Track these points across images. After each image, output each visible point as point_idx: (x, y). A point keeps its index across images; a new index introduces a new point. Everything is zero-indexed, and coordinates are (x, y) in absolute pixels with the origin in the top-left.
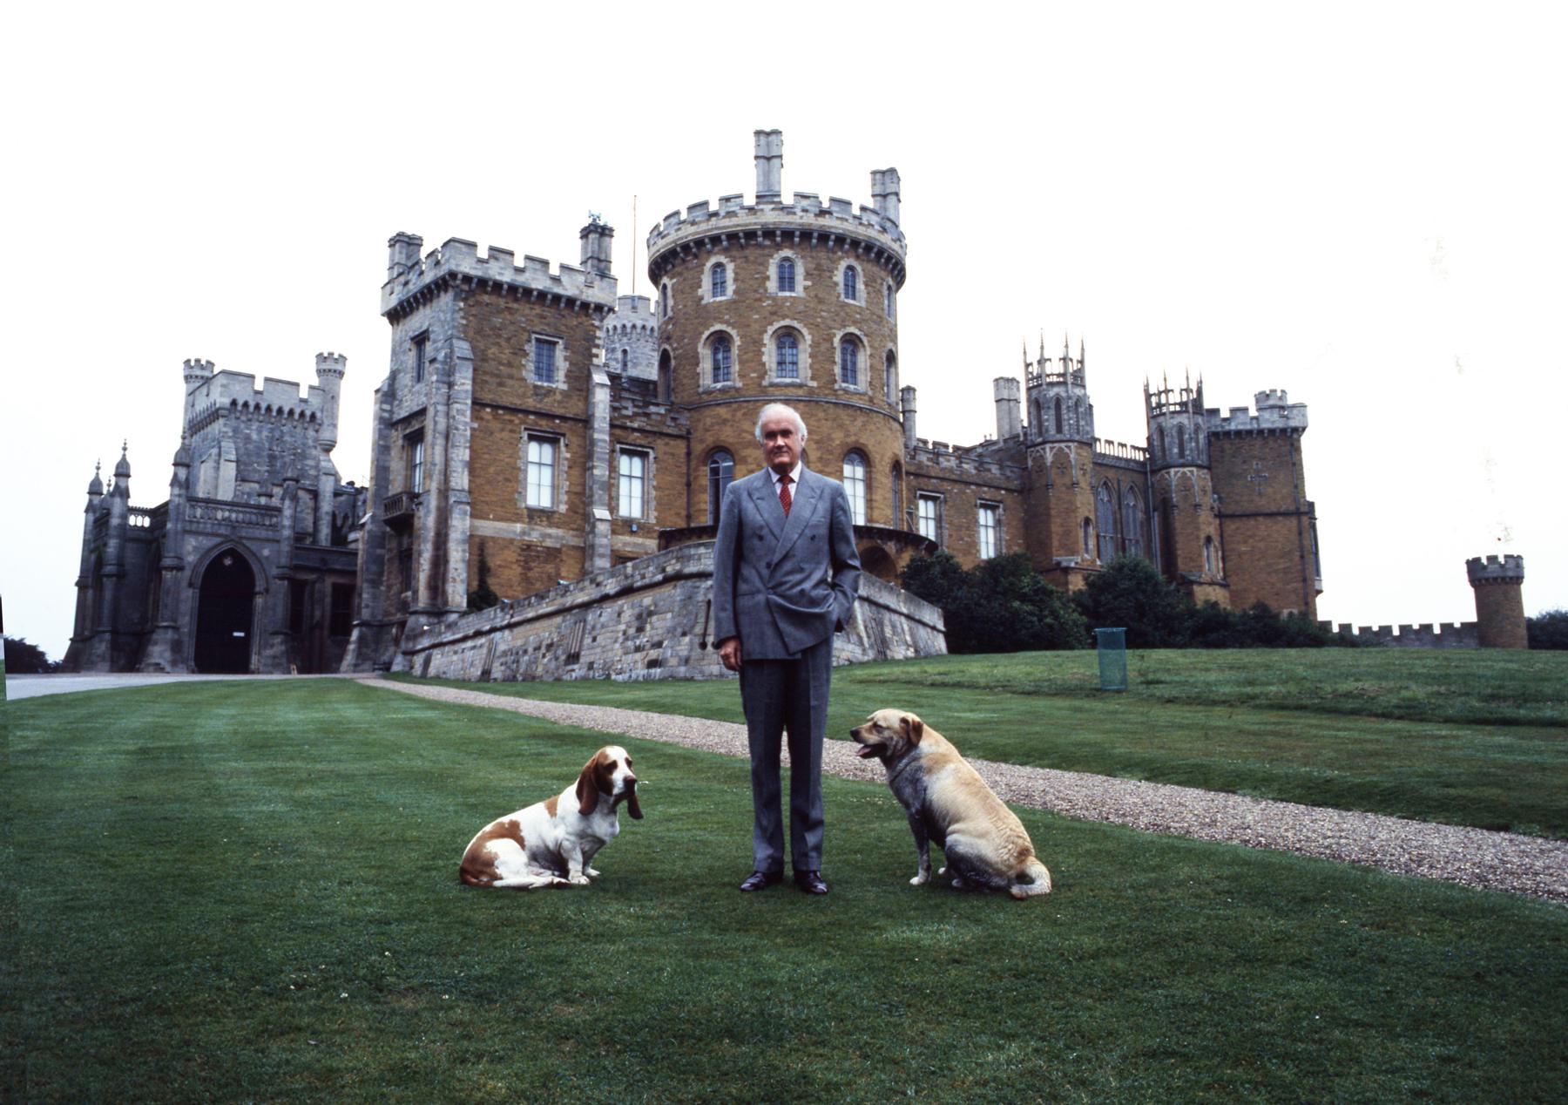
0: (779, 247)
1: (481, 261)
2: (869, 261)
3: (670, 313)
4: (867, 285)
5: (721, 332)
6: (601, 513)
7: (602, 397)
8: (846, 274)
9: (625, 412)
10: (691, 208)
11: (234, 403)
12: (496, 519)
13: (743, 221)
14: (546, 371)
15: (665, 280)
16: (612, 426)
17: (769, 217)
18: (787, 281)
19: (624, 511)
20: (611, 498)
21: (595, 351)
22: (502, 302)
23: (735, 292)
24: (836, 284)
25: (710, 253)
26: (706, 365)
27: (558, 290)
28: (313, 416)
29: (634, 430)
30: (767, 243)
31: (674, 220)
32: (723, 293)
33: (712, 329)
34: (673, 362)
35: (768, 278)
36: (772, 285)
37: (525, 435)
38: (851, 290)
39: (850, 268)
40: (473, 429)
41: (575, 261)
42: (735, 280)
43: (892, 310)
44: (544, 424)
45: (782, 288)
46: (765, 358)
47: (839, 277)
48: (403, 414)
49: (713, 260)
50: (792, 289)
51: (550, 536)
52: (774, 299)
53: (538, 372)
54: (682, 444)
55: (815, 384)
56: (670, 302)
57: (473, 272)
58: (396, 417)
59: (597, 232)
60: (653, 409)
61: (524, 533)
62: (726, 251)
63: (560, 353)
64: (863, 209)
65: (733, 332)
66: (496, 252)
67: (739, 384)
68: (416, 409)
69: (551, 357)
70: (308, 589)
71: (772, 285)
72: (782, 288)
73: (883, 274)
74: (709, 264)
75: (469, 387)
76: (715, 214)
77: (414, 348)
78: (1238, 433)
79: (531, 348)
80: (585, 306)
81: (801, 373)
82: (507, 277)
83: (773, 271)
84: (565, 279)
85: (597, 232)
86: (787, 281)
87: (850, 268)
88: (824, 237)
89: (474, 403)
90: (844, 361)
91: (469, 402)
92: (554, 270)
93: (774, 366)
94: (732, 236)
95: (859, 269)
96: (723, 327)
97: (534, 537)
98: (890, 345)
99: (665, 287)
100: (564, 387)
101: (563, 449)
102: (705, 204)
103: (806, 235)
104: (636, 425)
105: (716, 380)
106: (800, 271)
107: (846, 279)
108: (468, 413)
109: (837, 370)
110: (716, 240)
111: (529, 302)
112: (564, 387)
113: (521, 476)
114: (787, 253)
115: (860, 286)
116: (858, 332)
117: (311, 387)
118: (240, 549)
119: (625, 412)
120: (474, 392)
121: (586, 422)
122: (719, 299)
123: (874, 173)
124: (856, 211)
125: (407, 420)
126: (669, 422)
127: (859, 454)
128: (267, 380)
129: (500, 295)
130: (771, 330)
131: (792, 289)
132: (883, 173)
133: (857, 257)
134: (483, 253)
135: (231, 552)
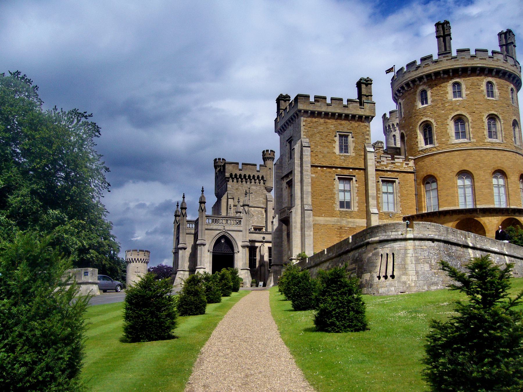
0: (452, 78)
1: (311, 103)
2: (500, 78)
3: (403, 116)
4: (499, 90)
5: (427, 121)
6: (373, 210)
7: (371, 159)
8: (487, 85)
9: (382, 163)
10: (408, 66)
11: (231, 175)
12: (325, 216)
13: (432, 68)
14: (344, 148)
15: (400, 101)
16: (376, 170)
17: (446, 65)
19: (385, 209)
20: (378, 203)
21: (366, 137)
22: (322, 121)
23: (432, 102)
24: (482, 91)
25: (419, 85)
27: (346, 112)
28: (263, 177)
29: (387, 171)
30: (446, 76)
31: (400, 72)
32: (427, 103)
33: (422, 121)
34: (406, 138)
35: (448, 93)
36: (450, 95)
37: (336, 177)
38: (491, 93)
39: (489, 83)
40: (312, 178)
41: (354, 96)
42: (431, 96)
43: (515, 100)
44: (346, 172)
45: (455, 96)
46: (448, 131)
47: (484, 87)
48: (286, 173)
49: (421, 88)
50: (460, 96)
51: (351, 222)
52: (451, 102)
53: (341, 150)
54: (412, 176)
55: (475, 140)
56: (403, 111)
57: (308, 109)
58: (284, 175)
59: (364, 84)
60: (396, 160)
61: (338, 221)
62: (424, 84)
63: (350, 139)
64: (494, 52)
65: (432, 121)
66: (318, 99)
67: (437, 145)
68: (290, 171)
69: (346, 142)
70: (258, 250)
72: (455, 96)
73: (508, 83)
74: (418, 91)
75: (309, 159)
76: (419, 67)
77: (288, 145)
79: (337, 139)
81: (468, 136)
82: (324, 109)
84: (350, 106)
85: (364, 84)
86: (457, 93)
87: (489, 83)
89: (312, 166)
90: (489, 128)
91: (310, 165)
92: (345, 103)
93: (454, 134)
94: (429, 76)
95: (494, 82)
96: (428, 119)
97: (344, 223)
98: (514, 118)
99: (400, 103)
100: (354, 154)
101: (355, 182)
102: (414, 62)
104: (388, 169)
105: (426, 144)
106: (463, 87)
107: (488, 88)
108: (309, 171)
109: (486, 133)
110: (420, 78)
111: (334, 119)
112: (354, 154)
113: (336, 196)
115: (496, 91)
116: (495, 113)
117: (261, 166)
118: (227, 235)
119: (382, 163)
120: (312, 162)
121: (365, 170)
122: (425, 105)
123: (500, 35)
124: (490, 54)
125: (287, 176)
126: (404, 165)
127: (500, 173)
128: (243, 164)
129: (341, 119)
130: (450, 117)
131: (460, 96)
132: (505, 34)
133: (492, 77)
134: (312, 99)
135: (223, 237)
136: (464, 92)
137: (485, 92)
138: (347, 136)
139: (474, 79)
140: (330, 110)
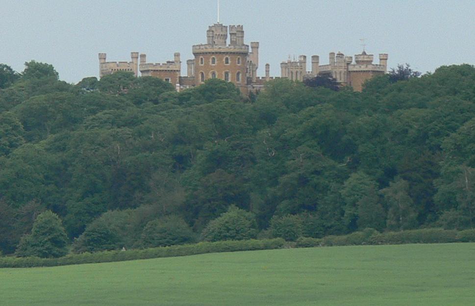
0: (212, 55)
18: (213, 62)
22: (158, 73)
26: (200, 78)
27: (169, 69)
36: (210, 63)
38: (227, 63)
47: (224, 60)
50: (214, 63)
52: (212, 66)
62: (202, 56)
71: (210, 63)
78: (357, 71)
80: (175, 71)
83: (211, 60)
88: (220, 53)
95: (229, 58)
103: (216, 53)
106: (216, 60)
114: (213, 56)
136: (216, 62)
137: (225, 62)
138: (168, 79)
139: (220, 56)
140: (161, 69)
